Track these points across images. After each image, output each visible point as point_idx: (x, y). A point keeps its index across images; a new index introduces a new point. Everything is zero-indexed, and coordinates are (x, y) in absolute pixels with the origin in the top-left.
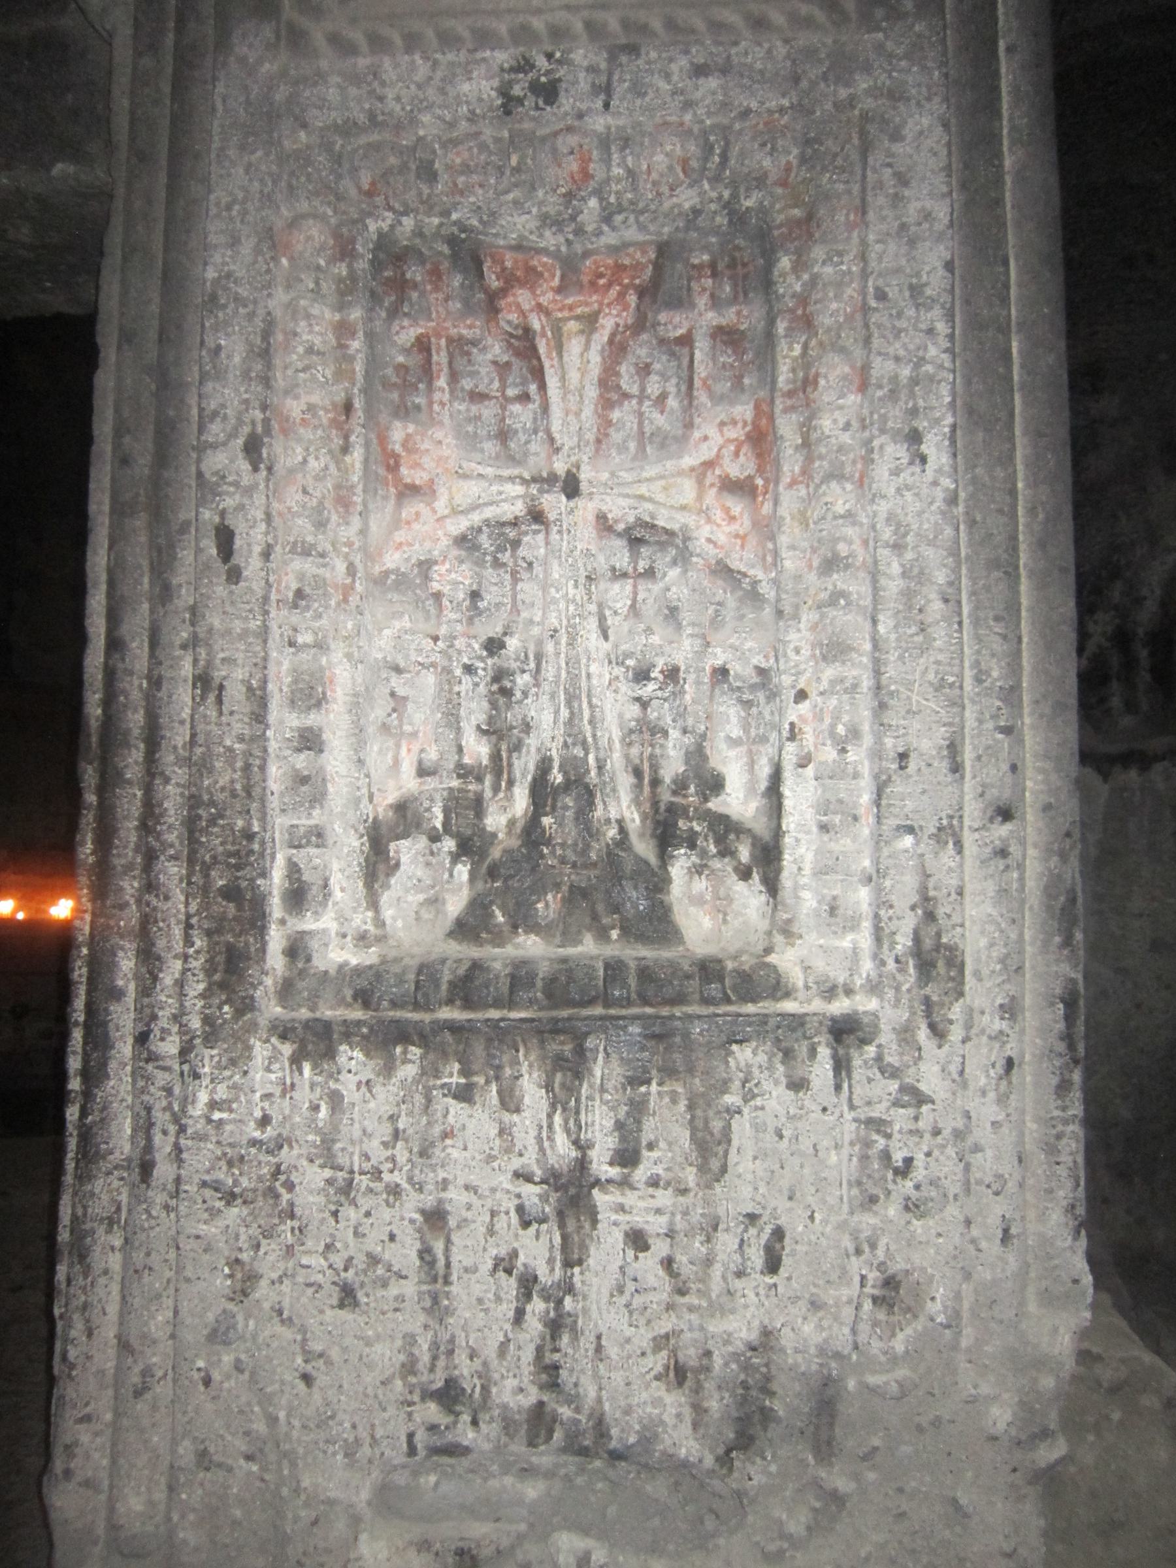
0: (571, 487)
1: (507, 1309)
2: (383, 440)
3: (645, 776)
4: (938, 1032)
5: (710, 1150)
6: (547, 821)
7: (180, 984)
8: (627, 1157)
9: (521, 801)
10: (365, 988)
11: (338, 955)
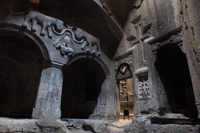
0: (144, 83)
5: (147, 102)
10: (139, 99)
11: (138, 98)
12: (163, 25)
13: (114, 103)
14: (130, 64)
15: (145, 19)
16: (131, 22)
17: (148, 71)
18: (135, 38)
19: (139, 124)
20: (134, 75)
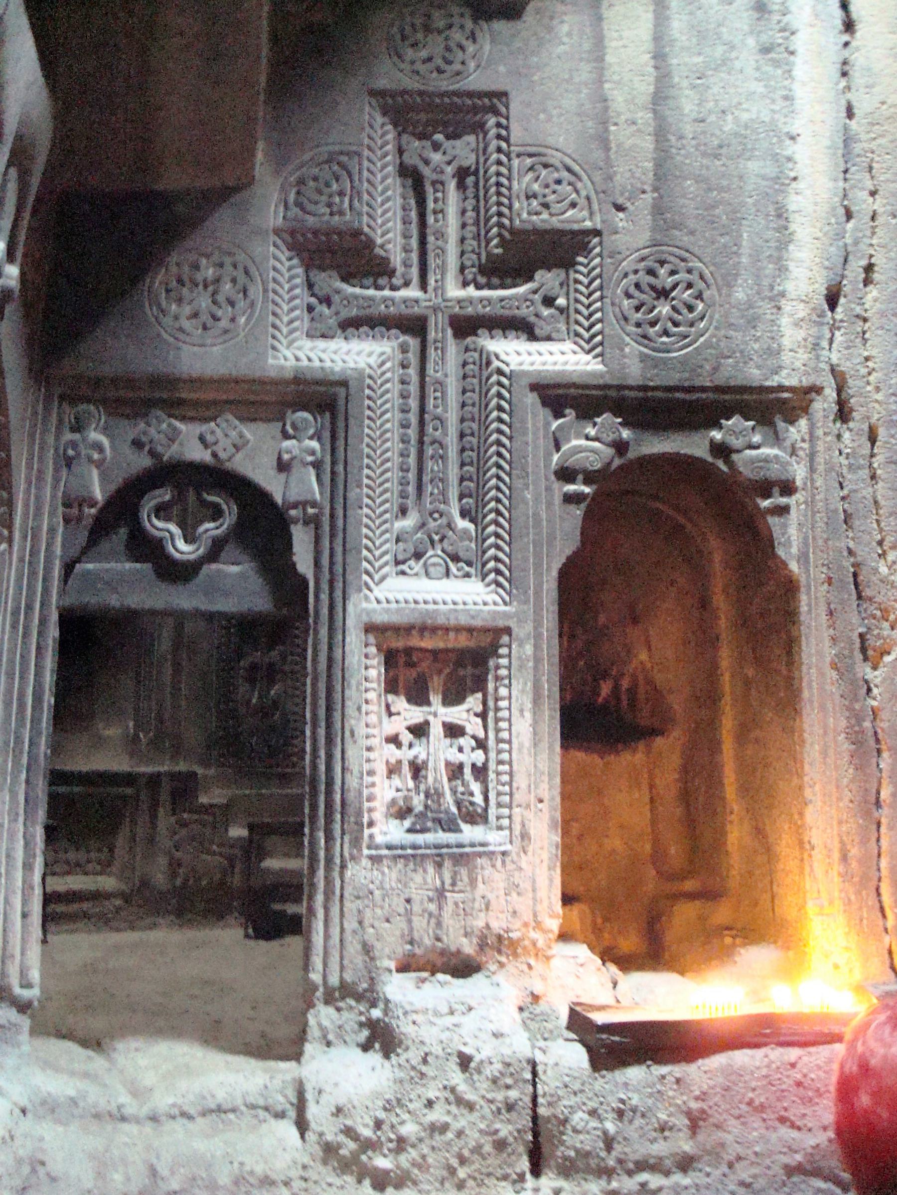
0: (435, 715)
1: (426, 921)
2: (386, 700)
3: (454, 792)
4: (525, 852)
5: (473, 882)
6: (429, 802)
7: (342, 845)
8: (454, 884)
9: (422, 796)
12: (691, 308)
13: (28, 867)
14: (295, 506)
15: (546, 166)
16: (373, 93)
17: (501, 623)
18: (377, 270)
19: (495, 1081)
20: (350, 622)
